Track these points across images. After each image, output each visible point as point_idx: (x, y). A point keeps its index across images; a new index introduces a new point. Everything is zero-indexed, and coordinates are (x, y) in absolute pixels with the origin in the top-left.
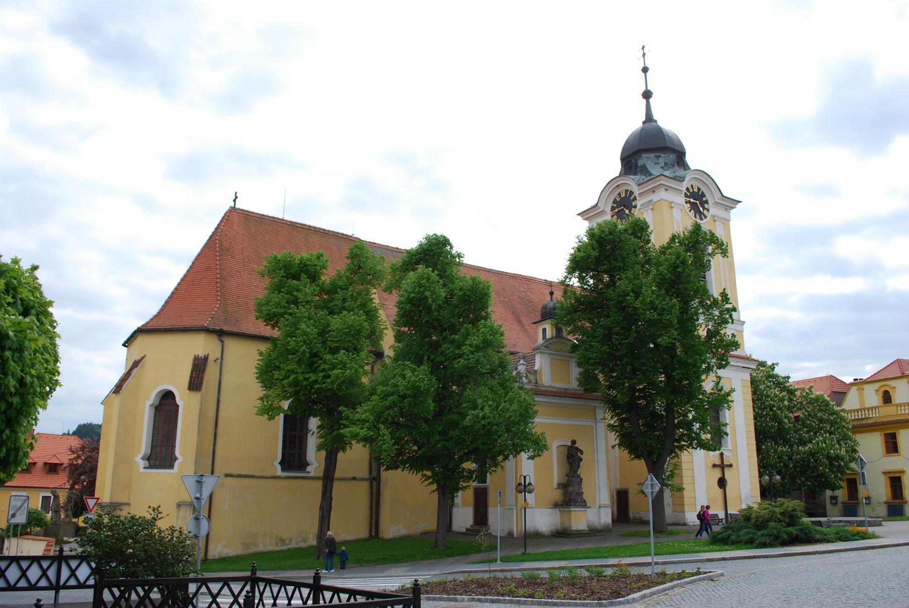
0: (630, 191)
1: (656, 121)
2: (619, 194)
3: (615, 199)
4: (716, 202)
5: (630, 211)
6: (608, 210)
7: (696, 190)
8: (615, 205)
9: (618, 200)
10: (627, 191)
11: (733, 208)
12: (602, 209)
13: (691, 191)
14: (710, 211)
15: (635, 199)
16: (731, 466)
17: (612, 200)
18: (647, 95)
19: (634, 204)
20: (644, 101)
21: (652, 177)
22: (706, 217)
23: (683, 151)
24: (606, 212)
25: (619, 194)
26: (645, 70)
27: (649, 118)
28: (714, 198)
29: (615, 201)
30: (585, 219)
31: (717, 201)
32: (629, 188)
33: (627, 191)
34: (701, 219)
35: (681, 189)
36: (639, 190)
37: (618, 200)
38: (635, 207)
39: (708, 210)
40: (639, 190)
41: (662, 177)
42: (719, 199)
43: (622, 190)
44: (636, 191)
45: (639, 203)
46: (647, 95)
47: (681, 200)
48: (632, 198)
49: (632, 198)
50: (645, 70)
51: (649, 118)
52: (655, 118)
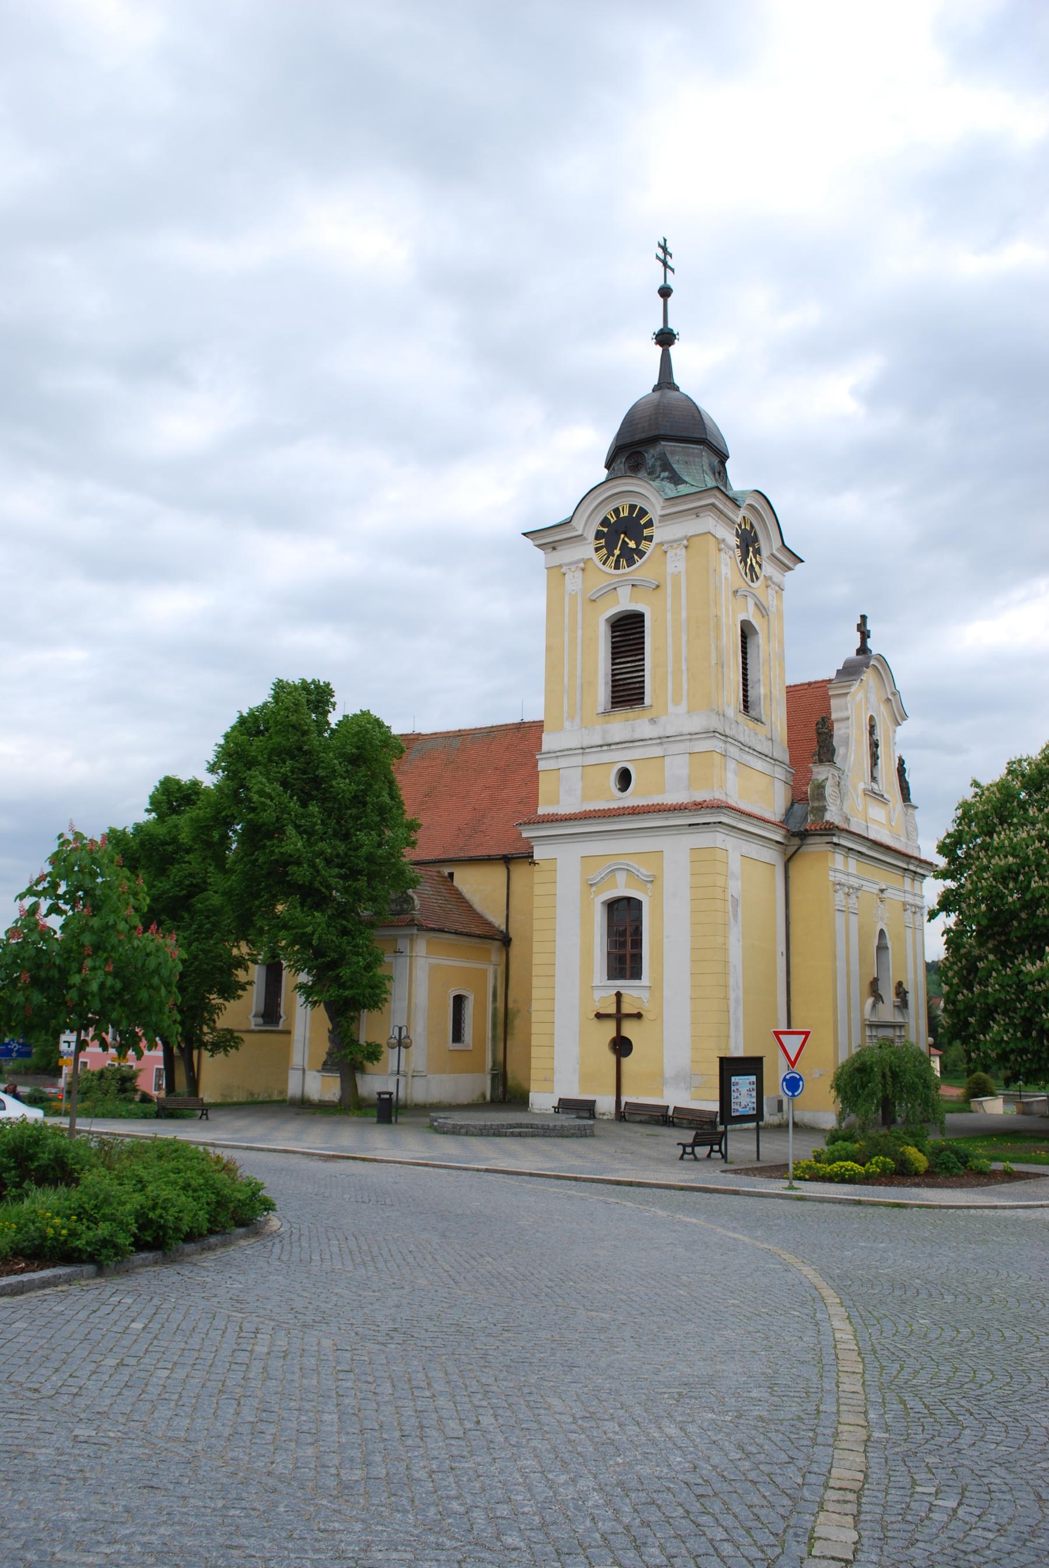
0: (641, 508)
2: (616, 511)
3: (606, 518)
4: (773, 555)
5: (638, 544)
6: (591, 535)
7: (748, 528)
8: (605, 530)
9: (612, 521)
10: (632, 507)
11: (790, 569)
12: (579, 533)
13: (743, 527)
14: (763, 567)
15: (650, 524)
16: (639, 1016)
17: (599, 519)
18: (665, 338)
19: (646, 532)
20: (659, 349)
21: (683, 489)
22: (757, 578)
23: (726, 453)
24: (585, 539)
25: (616, 511)
26: (665, 292)
28: (771, 546)
29: (605, 522)
30: (539, 546)
32: (640, 503)
33: (632, 507)
34: (753, 581)
35: (734, 517)
36: (663, 508)
37: (612, 521)
38: (650, 539)
39: (760, 566)
40: (663, 508)
42: (778, 550)
43: (623, 504)
44: (655, 508)
45: (660, 533)
47: (733, 541)
48: (642, 522)
49: (642, 522)
50: (665, 292)
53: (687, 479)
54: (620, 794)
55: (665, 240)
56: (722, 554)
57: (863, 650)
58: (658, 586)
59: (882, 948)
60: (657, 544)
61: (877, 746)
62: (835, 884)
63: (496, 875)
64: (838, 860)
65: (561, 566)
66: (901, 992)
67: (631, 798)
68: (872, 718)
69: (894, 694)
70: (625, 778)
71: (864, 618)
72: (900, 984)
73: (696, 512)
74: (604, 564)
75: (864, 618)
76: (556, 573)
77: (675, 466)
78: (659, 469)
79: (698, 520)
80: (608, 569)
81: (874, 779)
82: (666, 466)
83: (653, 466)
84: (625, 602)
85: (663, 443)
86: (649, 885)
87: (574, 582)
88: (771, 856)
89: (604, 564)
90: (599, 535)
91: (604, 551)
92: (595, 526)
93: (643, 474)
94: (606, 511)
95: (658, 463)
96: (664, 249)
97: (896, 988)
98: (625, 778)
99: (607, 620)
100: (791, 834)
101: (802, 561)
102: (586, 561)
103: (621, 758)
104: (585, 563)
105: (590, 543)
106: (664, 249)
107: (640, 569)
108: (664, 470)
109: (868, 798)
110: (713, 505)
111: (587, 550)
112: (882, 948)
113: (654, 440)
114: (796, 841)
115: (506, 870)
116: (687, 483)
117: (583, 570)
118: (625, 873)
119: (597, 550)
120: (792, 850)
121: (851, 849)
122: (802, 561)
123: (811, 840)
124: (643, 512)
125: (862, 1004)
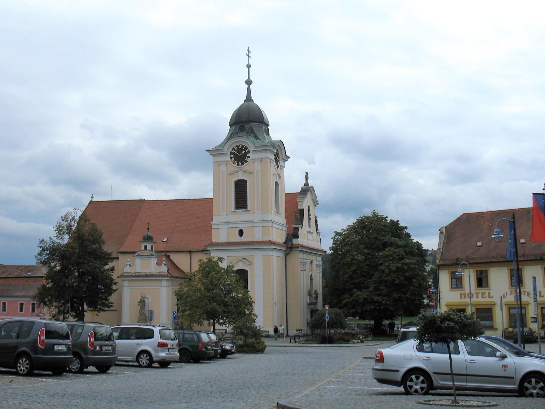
1: (252, 101)
2: (237, 146)
12: (226, 152)
17: (232, 148)
18: (249, 83)
27: (249, 99)
31: (283, 157)
32: (245, 145)
33: (243, 146)
36: (254, 148)
38: (249, 157)
40: (254, 148)
41: (271, 146)
44: (251, 148)
45: (252, 156)
46: (249, 83)
50: (249, 66)
51: (249, 99)
52: (252, 98)
53: (260, 137)
54: (240, 237)
55: (249, 48)
56: (272, 163)
57: (306, 184)
58: (252, 173)
59: (311, 280)
60: (251, 159)
61: (310, 215)
62: (300, 263)
63: (186, 257)
64: (301, 255)
65: (218, 162)
66: (316, 293)
67: (243, 239)
68: (309, 206)
69: (315, 197)
70: (241, 233)
71: (307, 173)
72: (316, 291)
73: (266, 151)
74: (233, 163)
75: (307, 173)
76: (217, 164)
77: (255, 132)
78: (250, 132)
79: (267, 153)
80: (234, 165)
81: (309, 226)
82: (253, 132)
83: (248, 131)
84: (240, 176)
85: (251, 123)
86: (250, 266)
87: (223, 168)
88: (281, 254)
89: (233, 163)
90: (231, 153)
91: (233, 159)
92: (230, 150)
93: (244, 133)
94: (234, 146)
95: (250, 130)
96: (248, 51)
97: (315, 292)
98: (241, 233)
99: (234, 182)
100: (287, 248)
101: (290, 158)
102: (227, 161)
103: (241, 226)
104: (227, 162)
105: (229, 156)
106: (248, 51)
107: (247, 166)
108: (252, 133)
109: (308, 233)
110: (270, 149)
111: (228, 158)
112: (311, 280)
113: (248, 122)
114: (289, 250)
115: (190, 256)
116: (260, 139)
117: (226, 164)
118: (242, 262)
119: (231, 158)
120: (288, 252)
121: (304, 251)
122: (290, 158)
123: (294, 249)
124: (246, 148)
125: (307, 298)
